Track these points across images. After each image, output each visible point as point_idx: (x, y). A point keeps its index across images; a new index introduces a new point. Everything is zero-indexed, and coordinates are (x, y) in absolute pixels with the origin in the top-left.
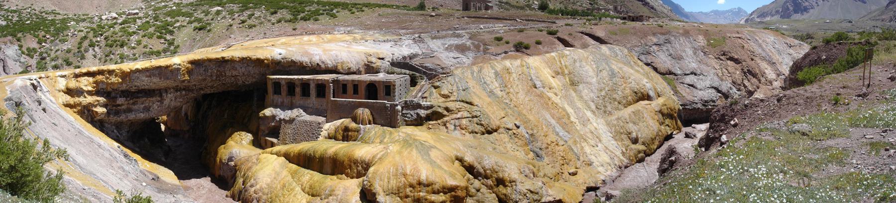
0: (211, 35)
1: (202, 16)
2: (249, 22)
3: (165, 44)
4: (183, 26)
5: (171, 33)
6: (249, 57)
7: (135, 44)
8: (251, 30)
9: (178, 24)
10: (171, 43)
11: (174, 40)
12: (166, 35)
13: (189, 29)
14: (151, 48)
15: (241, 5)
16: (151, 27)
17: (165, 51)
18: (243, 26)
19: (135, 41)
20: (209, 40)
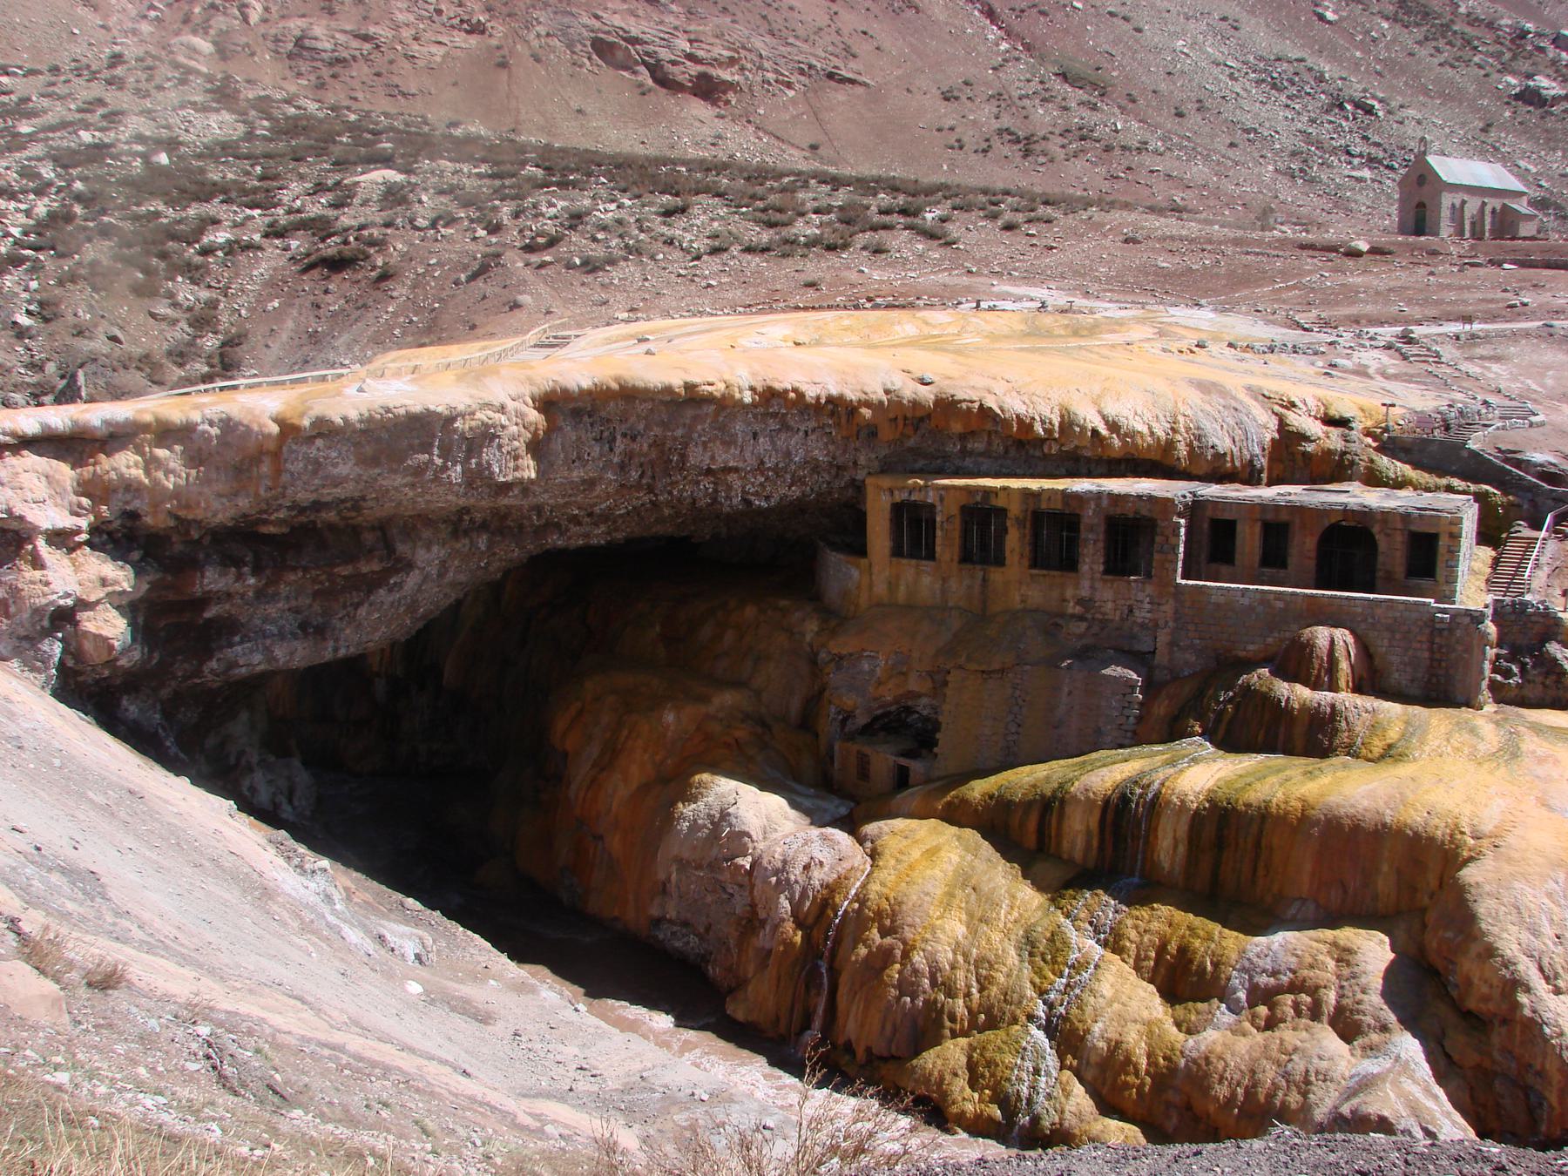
0: (400, 291)
1: (317, 208)
2: (577, 245)
3: (174, 322)
4: (250, 246)
5: (194, 273)
6: (795, 390)
7: (29, 312)
8: (589, 279)
9: (221, 237)
10: (203, 320)
11: (212, 305)
12: (173, 279)
13: (270, 261)
14: (114, 339)
15: (483, 169)
16: (89, 240)
17: (180, 356)
18: (558, 261)
19: (29, 302)
20: (395, 314)
